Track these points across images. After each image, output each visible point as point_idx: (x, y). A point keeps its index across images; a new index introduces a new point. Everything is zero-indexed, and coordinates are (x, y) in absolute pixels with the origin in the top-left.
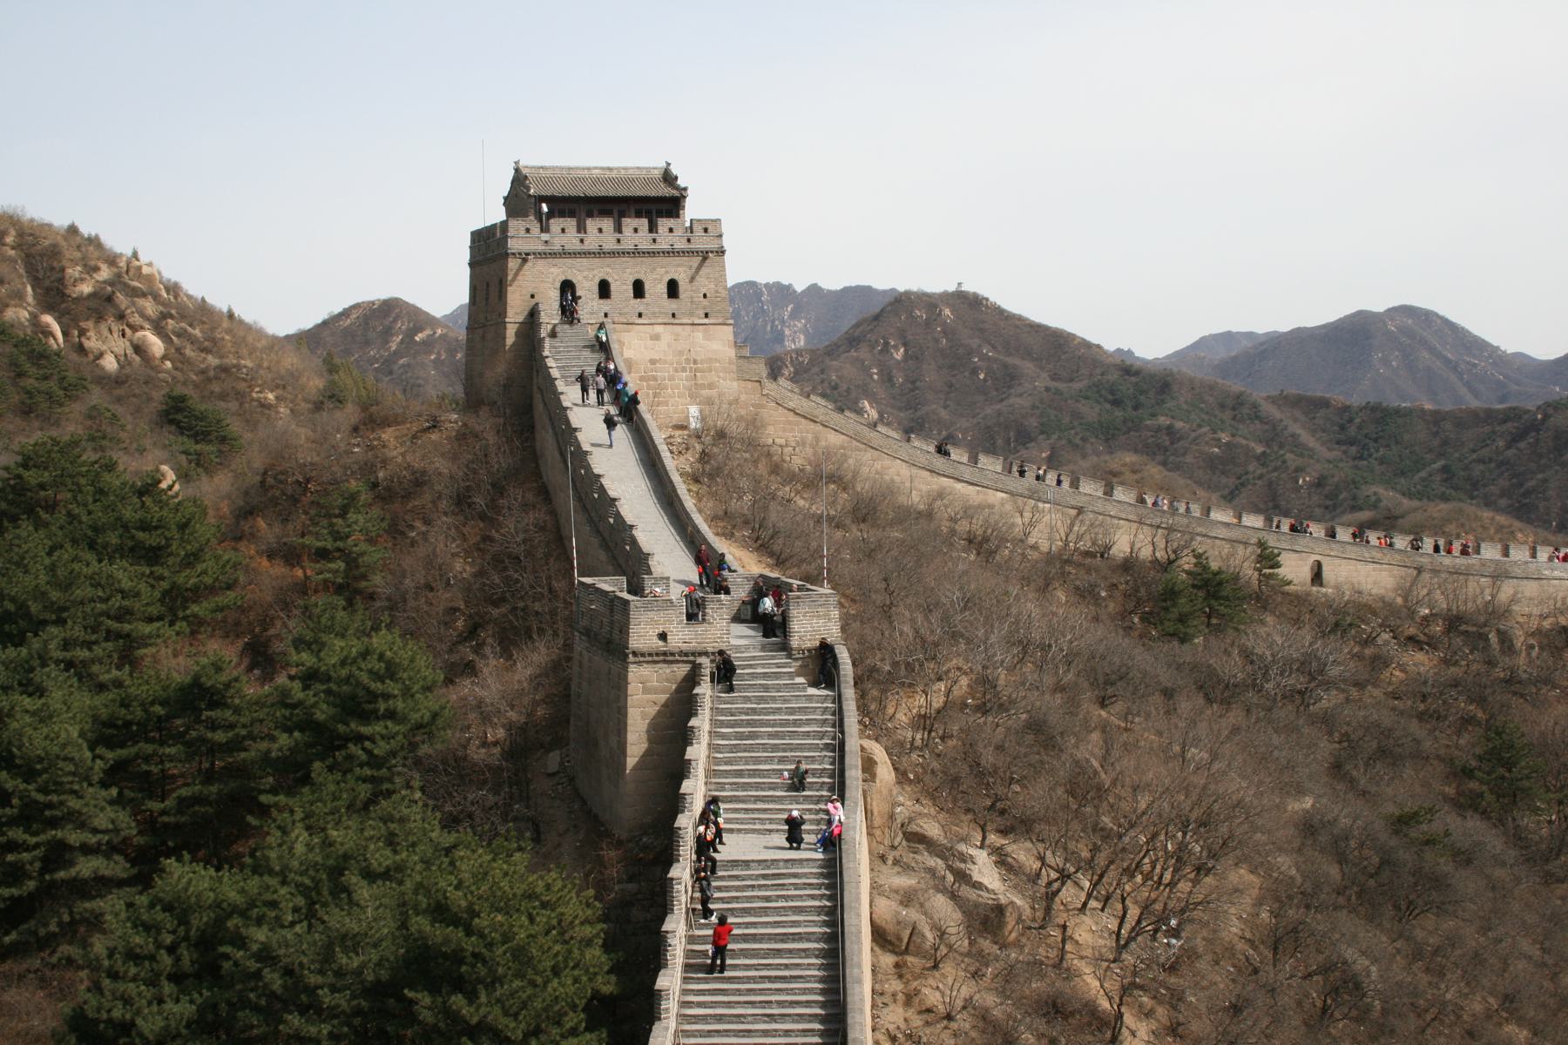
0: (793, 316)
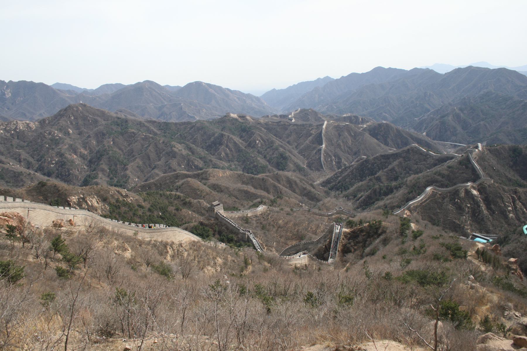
0: (7, 88)
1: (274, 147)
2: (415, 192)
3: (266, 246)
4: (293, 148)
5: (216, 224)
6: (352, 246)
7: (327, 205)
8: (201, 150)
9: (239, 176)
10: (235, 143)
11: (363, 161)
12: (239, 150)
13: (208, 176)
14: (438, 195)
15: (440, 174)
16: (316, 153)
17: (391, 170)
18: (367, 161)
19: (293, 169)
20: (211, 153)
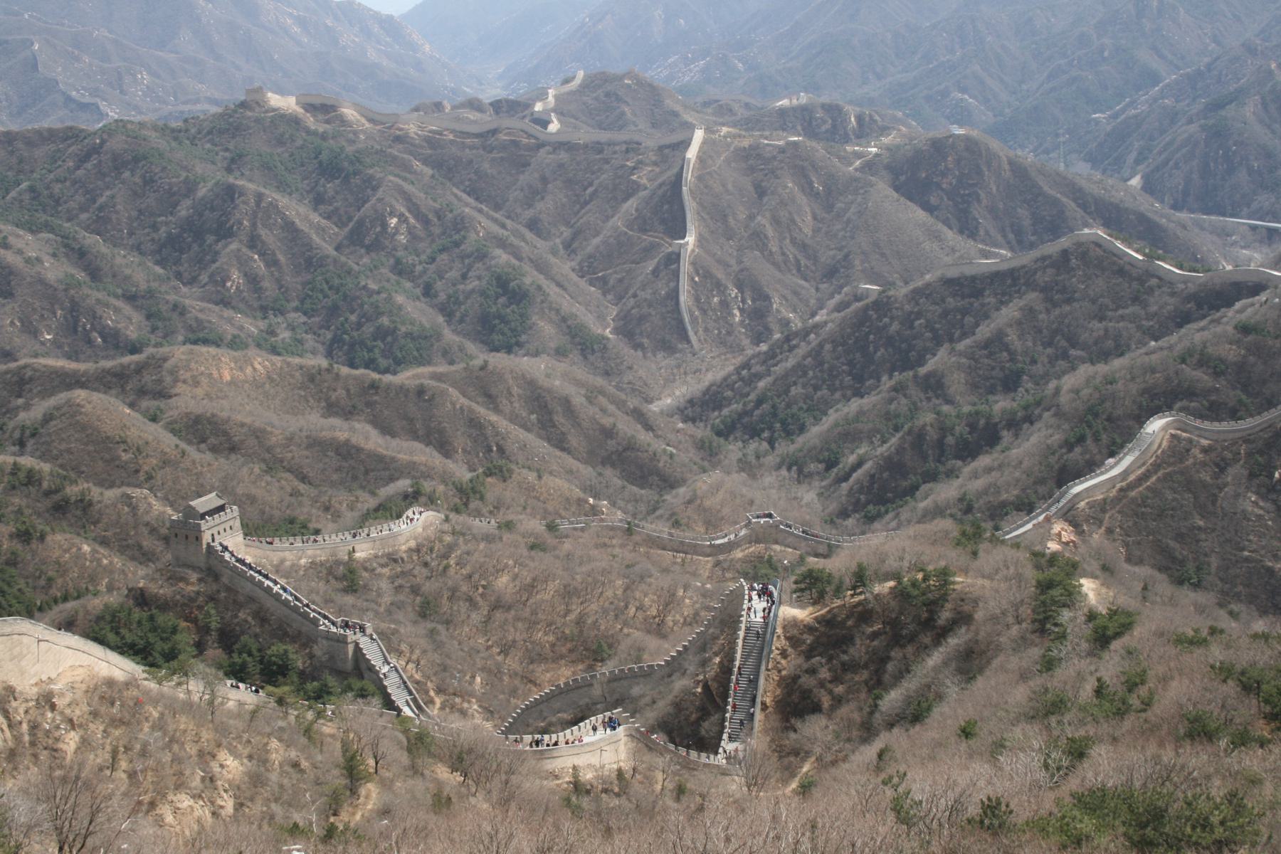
1: (467, 247)
2: (1097, 439)
3: (439, 691)
4: (554, 252)
5: (212, 598)
6: (822, 684)
7: (707, 503)
8: (134, 258)
9: (312, 379)
10: (290, 227)
11: (866, 308)
12: (309, 261)
13: (168, 379)
14: (1196, 451)
15: (1204, 361)
16: (655, 272)
17: (987, 344)
18: (882, 306)
19: (553, 345)
20: (179, 276)
